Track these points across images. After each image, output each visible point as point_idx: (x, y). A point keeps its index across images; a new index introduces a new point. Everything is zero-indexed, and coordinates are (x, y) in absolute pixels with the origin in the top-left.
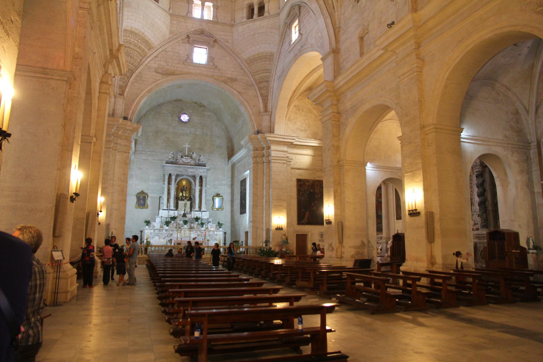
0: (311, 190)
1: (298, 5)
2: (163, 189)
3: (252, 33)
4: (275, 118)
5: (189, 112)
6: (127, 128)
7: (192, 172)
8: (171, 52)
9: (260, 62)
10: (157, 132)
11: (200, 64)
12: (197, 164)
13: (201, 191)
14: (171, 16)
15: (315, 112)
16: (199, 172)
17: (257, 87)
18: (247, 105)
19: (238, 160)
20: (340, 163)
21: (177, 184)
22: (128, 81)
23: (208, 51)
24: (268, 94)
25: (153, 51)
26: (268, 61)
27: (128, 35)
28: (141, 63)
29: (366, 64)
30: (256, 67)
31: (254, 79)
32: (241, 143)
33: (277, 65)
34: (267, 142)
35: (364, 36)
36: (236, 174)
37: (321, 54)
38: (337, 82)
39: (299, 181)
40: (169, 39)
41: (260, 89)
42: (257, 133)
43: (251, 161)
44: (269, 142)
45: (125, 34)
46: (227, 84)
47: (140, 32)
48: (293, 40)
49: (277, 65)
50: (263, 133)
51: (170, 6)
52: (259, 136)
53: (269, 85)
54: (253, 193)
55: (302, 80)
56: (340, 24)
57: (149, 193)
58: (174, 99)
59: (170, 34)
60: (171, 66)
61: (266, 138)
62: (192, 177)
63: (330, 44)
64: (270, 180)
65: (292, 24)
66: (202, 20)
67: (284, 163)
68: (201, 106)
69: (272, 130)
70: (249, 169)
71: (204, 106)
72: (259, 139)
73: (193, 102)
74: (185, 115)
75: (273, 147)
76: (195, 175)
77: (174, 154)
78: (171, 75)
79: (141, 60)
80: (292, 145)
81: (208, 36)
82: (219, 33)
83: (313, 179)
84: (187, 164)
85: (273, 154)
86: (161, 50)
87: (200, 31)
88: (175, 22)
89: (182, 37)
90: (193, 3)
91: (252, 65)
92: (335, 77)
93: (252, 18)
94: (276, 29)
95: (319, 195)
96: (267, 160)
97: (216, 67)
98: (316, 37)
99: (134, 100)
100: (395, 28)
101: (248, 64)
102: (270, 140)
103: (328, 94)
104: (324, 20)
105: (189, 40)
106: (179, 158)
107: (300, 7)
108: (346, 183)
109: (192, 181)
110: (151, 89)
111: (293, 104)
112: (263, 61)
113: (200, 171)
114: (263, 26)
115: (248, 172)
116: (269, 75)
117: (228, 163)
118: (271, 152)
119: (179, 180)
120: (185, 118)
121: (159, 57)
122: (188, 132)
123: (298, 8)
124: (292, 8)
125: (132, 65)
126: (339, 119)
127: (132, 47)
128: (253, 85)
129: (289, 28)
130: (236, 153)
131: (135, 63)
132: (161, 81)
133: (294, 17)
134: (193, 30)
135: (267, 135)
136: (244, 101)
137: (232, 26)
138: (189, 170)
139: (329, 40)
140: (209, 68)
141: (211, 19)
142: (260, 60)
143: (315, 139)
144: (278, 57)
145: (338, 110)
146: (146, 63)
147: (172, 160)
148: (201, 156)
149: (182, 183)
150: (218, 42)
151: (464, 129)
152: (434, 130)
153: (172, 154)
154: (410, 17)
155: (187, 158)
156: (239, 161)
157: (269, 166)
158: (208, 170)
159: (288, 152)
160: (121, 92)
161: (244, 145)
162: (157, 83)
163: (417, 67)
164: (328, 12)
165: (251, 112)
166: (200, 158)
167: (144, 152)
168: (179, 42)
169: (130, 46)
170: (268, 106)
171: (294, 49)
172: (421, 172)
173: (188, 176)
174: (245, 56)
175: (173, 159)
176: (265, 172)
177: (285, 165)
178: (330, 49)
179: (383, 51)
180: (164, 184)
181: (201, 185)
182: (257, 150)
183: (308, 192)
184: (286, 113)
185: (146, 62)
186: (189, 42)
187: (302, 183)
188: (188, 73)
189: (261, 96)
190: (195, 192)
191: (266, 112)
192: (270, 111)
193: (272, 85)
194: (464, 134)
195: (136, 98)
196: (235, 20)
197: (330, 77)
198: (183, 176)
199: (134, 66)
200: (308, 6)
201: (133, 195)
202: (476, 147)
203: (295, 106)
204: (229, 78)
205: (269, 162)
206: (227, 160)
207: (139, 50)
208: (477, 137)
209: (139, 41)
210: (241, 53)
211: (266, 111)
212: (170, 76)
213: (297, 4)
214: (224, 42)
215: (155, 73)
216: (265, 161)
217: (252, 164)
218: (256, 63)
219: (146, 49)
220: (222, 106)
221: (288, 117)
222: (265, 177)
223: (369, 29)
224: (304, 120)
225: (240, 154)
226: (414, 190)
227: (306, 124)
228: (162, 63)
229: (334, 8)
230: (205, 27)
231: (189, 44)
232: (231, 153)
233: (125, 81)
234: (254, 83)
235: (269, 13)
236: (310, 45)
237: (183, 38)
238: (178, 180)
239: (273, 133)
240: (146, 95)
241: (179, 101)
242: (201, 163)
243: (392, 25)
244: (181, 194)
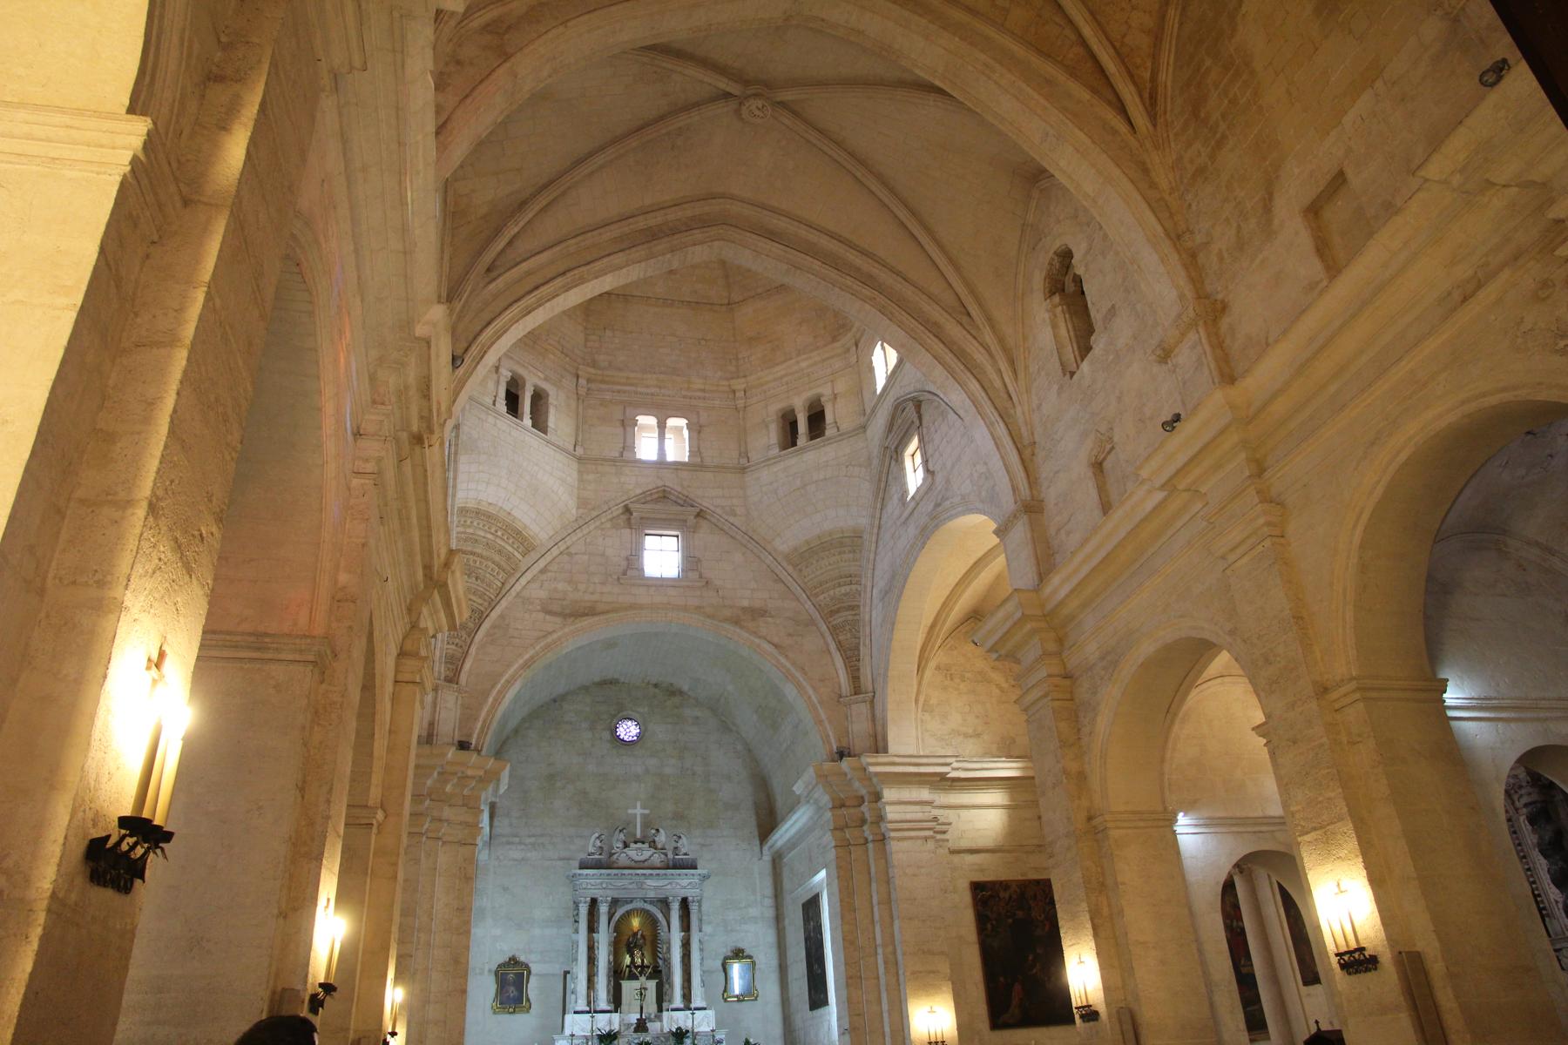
0: (1020, 914)
1: (912, 399)
2: (575, 946)
3: (798, 482)
4: (884, 710)
5: (638, 712)
6: (469, 772)
7: (656, 888)
8: (584, 554)
9: (828, 557)
10: (551, 777)
11: (662, 579)
12: (671, 864)
13: (686, 945)
14: (579, 463)
15: (997, 677)
16: (678, 887)
17: (825, 627)
18: (801, 679)
19: (789, 840)
20: (1095, 822)
21: (617, 929)
22: (469, 641)
23: (683, 541)
24: (859, 644)
25: (534, 556)
26: (850, 552)
27: (468, 523)
28: (504, 592)
29: (1122, 533)
30: (819, 573)
31: (813, 604)
32: (794, 788)
33: (875, 560)
34: (870, 779)
35: (1104, 459)
36: (787, 885)
37: (995, 520)
38: (1048, 590)
39: (977, 887)
40: (576, 520)
41: (835, 630)
42: (836, 756)
43: (829, 839)
44: (875, 780)
45: (463, 520)
46: (742, 627)
47: (502, 511)
48: (912, 489)
49: (875, 560)
50: (855, 756)
51: (577, 435)
52: (846, 764)
53: (857, 617)
54: (844, 939)
55: (948, 593)
56: (1033, 434)
57: (535, 962)
58: (597, 679)
59: (578, 508)
60: (585, 592)
61: (865, 769)
62: (659, 904)
63: (1014, 490)
64: (889, 894)
65: (906, 446)
66: (661, 464)
67: (926, 839)
68: (673, 692)
69: (880, 744)
70: (826, 866)
71: (681, 693)
72: (846, 774)
73: (648, 683)
74: (629, 723)
75: (889, 794)
76: (668, 898)
77: (603, 837)
78: (587, 615)
79: (503, 584)
80: (942, 782)
81: (682, 502)
82: (709, 494)
83: (1020, 878)
84: (642, 865)
85: (892, 813)
86: (555, 552)
87: (657, 492)
88: (591, 477)
89: (612, 513)
90: (636, 425)
91: (807, 567)
92: (1042, 577)
93: (794, 444)
94: (860, 466)
95: (1047, 928)
96: (876, 834)
97: (707, 582)
98: (972, 474)
99: (486, 694)
100: (1186, 429)
101: (795, 566)
102: (877, 774)
103: (1028, 627)
104: (989, 430)
105: (629, 519)
106: (618, 850)
107: (918, 405)
108: (1123, 884)
109: (660, 916)
110: (532, 657)
111: (932, 664)
112: (834, 555)
113: (681, 884)
114: (827, 461)
115: (822, 874)
116: (857, 590)
117: (761, 848)
118: (884, 807)
119: (621, 917)
120: (628, 730)
121: (551, 571)
122: (639, 770)
124: (899, 408)
125: (480, 598)
126: (1071, 692)
127: (478, 551)
128: (812, 622)
129: (897, 461)
130: (784, 819)
131: (488, 593)
132: (559, 634)
133: (907, 431)
134: (638, 491)
135: (867, 759)
136: (792, 669)
137: (743, 470)
138: (649, 882)
139: (1011, 480)
140: (688, 587)
141: (687, 460)
142: (827, 553)
143: (1007, 757)
144: (874, 539)
145: (1065, 668)
146: (518, 590)
147: (596, 857)
148: (680, 837)
149: (631, 923)
150: (708, 517)
151: (1448, 680)
152: (1357, 696)
153: (598, 838)
154: (1219, 396)
155: (640, 849)
156: (793, 844)
157: (885, 850)
158: (705, 878)
159: (935, 804)
161: (805, 794)
162: (549, 639)
163: (1268, 524)
164: (996, 408)
165: (813, 698)
166: (679, 845)
167: (517, 840)
168: (603, 526)
169: (475, 550)
170: (861, 677)
172: (1347, 827)
173: (645, 902)
174: (783, 545)
175: (600, 854)
176: (873, 870)
177: (931, 845)
178: (1016, 503)
179: (1165, 493)
180: (577, 931)
181: (686, 927)
182: (842, 806)
183: (1010, 921)
184: (915, 690)
185: (518, 587)
186: (629, 524)
187: (989, 893)
188: (632, 607)
189: (840, 651)
190: (669, 949)
191: (858, 694)
192: (871, 689)
193: (867, 617)
194: (1452, 696)
195: (493, 686)
196: (749, 455)
197: (1027, 577)
198: (631, 902)
199: (485, 600)
200: (938, 399)
201: (486, 972)
202: (1500, 732)
203: (938, 668)
204: (744, 609)
205: (882, 839)
206: (758, 843)
207: (497, 558)
208: (1495, 699)
209: (499, 533)
210: (773, 540)
211: (857, 690)
212: (584, 618)
213: (909, 396)
214: (724, 516)
215: (541, 615)
216: (870, 838)
217: (833, 850)
218: (817, 561)
219: (516, 553)
220: (730, 688)
221: (922, 699)
222: (874, 886)
223: (1116, 439)
224: (969, 705)
225: (795, 822)
226: (1338, 885)
227: (977, 717)
228: (561, 586)
229: (1011, 398)
230: (671, 481)
231: (631, 528)
232: (767, 823)
233: (460, 643)
234: (816, 616)
235: (838, 428)
236: (959, 498)
237: (615, 514)
238: (617, 916)
239: (885, 750)
240: (520, 676)
241: (611, 683)
242: (682, 859)
243: (1175, 425)
244: (628, 960)
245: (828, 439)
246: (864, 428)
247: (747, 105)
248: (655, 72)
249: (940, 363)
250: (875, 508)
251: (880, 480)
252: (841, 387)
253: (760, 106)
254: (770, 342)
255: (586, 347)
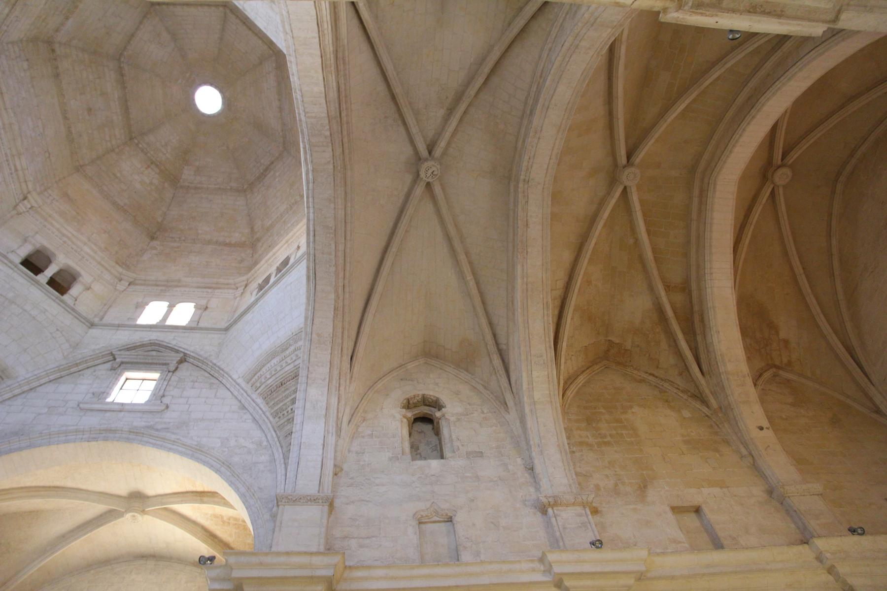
3: (11, 295)
48: (109, 400)
123: (179, 358)
144: (17, 392)
171: (108, 414)
245: (62, 301)
246: (92, 325)
247: (436, 165)
248: (447, 98)
249: (330, 369)
250: (48, 375)
251: (77, 365)
252: (97, 287)
253: (435, 173)
254: (77, 213)
255: (7, 43)
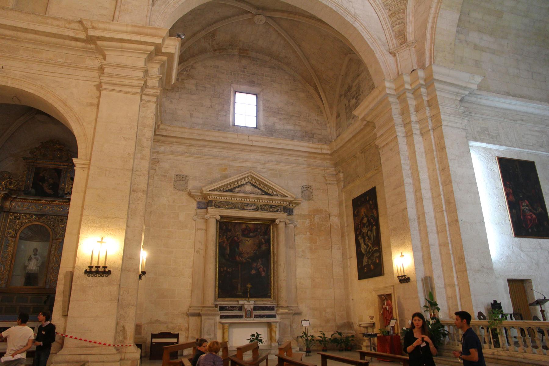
160: (403, 40)
